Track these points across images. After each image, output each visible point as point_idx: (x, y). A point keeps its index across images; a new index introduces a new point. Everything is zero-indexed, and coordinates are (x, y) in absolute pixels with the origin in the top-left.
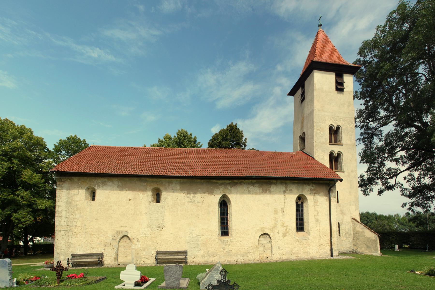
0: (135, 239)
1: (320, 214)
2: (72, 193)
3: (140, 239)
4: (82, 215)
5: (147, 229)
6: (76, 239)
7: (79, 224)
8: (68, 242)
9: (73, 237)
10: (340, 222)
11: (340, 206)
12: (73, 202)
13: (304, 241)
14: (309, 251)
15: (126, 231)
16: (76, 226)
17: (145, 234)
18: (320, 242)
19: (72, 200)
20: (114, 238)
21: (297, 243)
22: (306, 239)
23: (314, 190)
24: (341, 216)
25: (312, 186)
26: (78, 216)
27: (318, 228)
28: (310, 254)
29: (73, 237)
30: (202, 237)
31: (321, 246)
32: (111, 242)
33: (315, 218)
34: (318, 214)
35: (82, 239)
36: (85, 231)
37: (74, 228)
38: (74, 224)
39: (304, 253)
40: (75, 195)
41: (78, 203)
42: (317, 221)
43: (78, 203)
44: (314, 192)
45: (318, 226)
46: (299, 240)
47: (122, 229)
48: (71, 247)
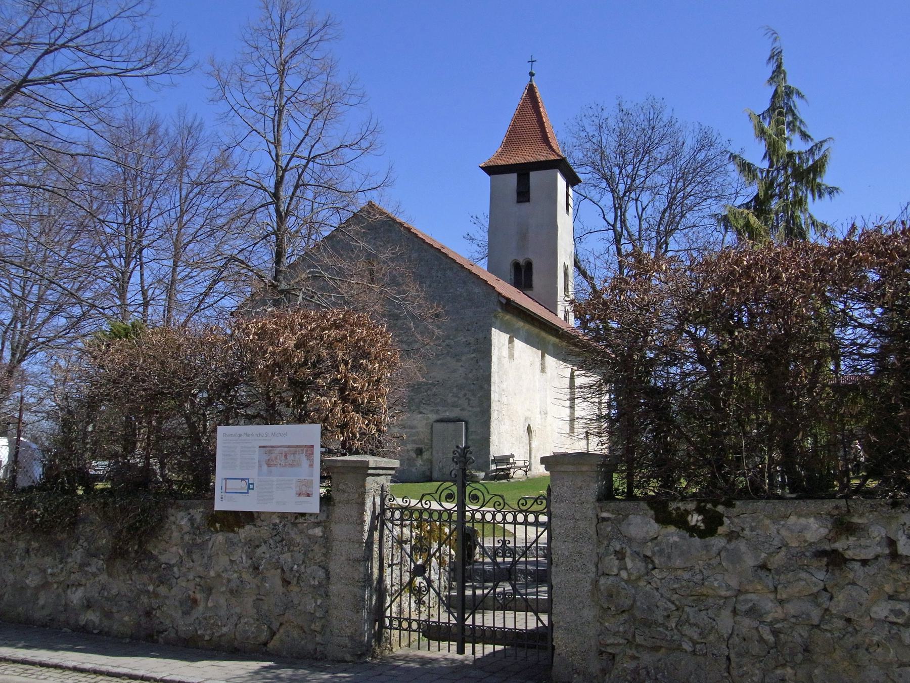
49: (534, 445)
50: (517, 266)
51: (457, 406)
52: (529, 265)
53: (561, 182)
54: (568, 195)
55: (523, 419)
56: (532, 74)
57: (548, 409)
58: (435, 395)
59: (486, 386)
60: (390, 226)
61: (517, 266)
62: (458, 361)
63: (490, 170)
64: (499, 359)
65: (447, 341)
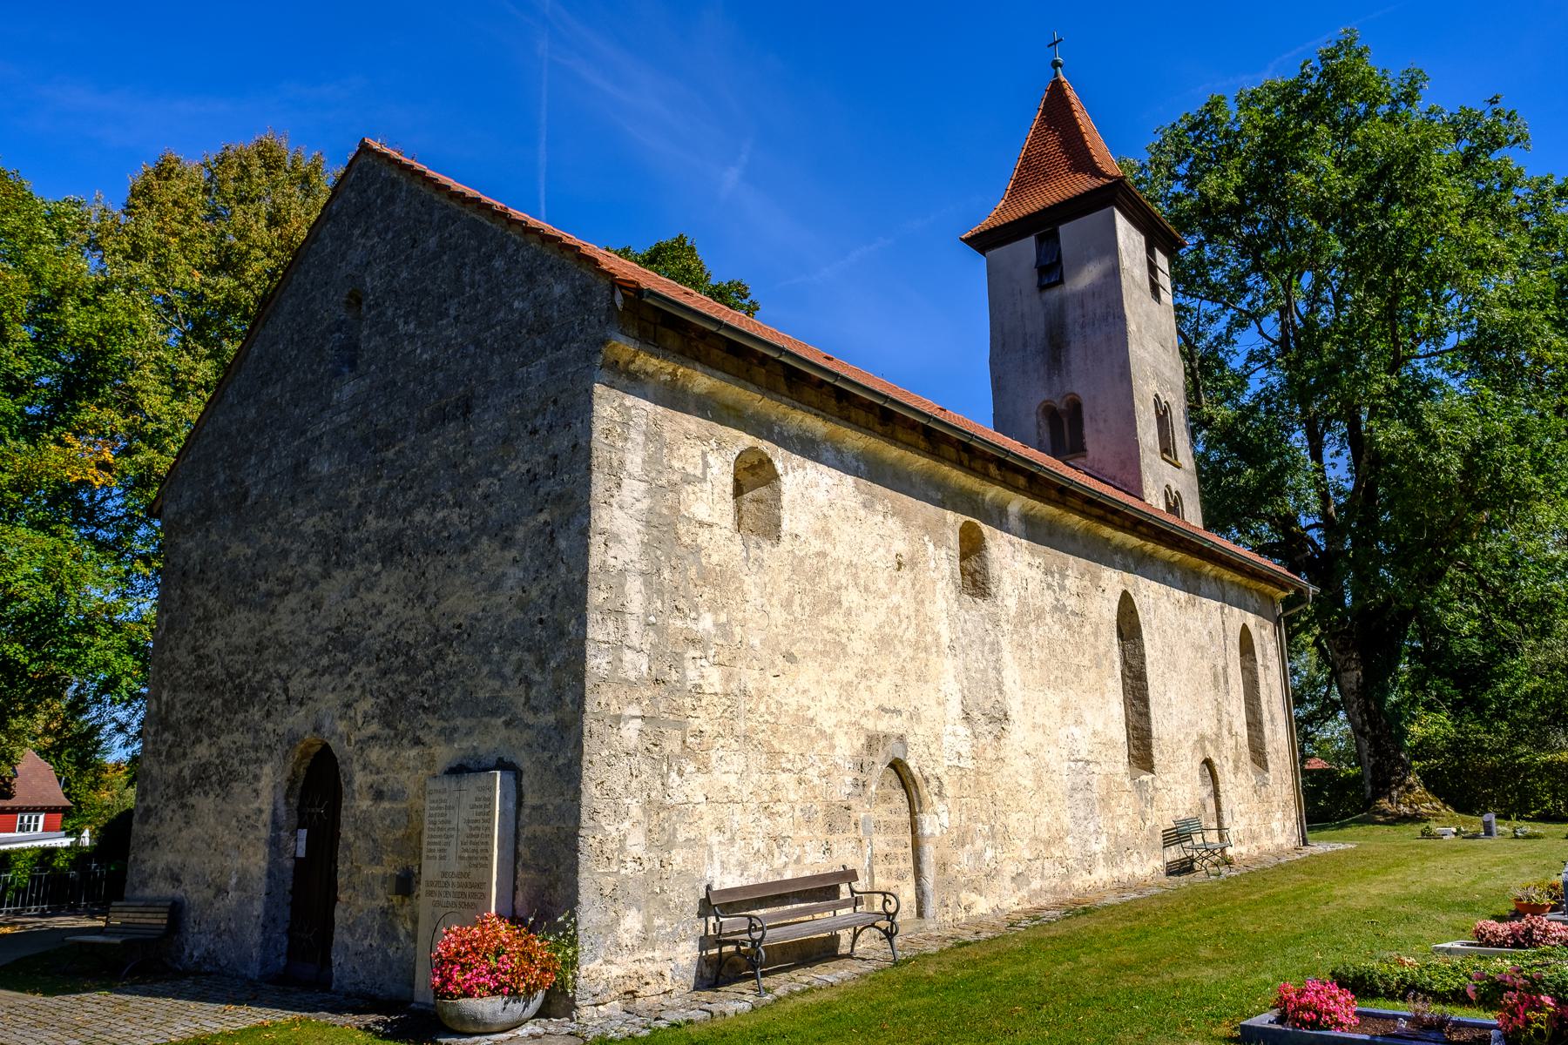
0: (934, 783)
2: (676, 464)
3: (945, 779)
4: (723, 618)
5: (963, 730)
6: (702, 779)
7: (714, 679)
8: (662, 807)
9: (690, 767)
12: (682, 528)
15: (901, 738)
16: (698, 691)
17: (960, 755)
19: (675, 510)
20: (862, 777)
26: (706, 623)
29: (690, 767)
30: (1097, 769)
32: (852, 802)
35: (732, 780)
36: (741, 726)
37: (688, 701)
38: (692, 674)
40: (688, 479)
41: (703, 536)
43: (703, 536)
47: (883, 725)
48: (681, 836)
49: (931, 825)
50: (1051, 415)
51: (494, 713)
52: (1075, 408)
53: (1129, 238)
54: (1153, 268)
55: (847, 746)
56: (1056, 64)
57: (1014, 707)
58: (449, 676)
59: (572, 627)
60: (394, 183)
61: (1051, 415)
62: (507, 543)
63: (983, 242)
64: (664, 529)
65: (484, 482)
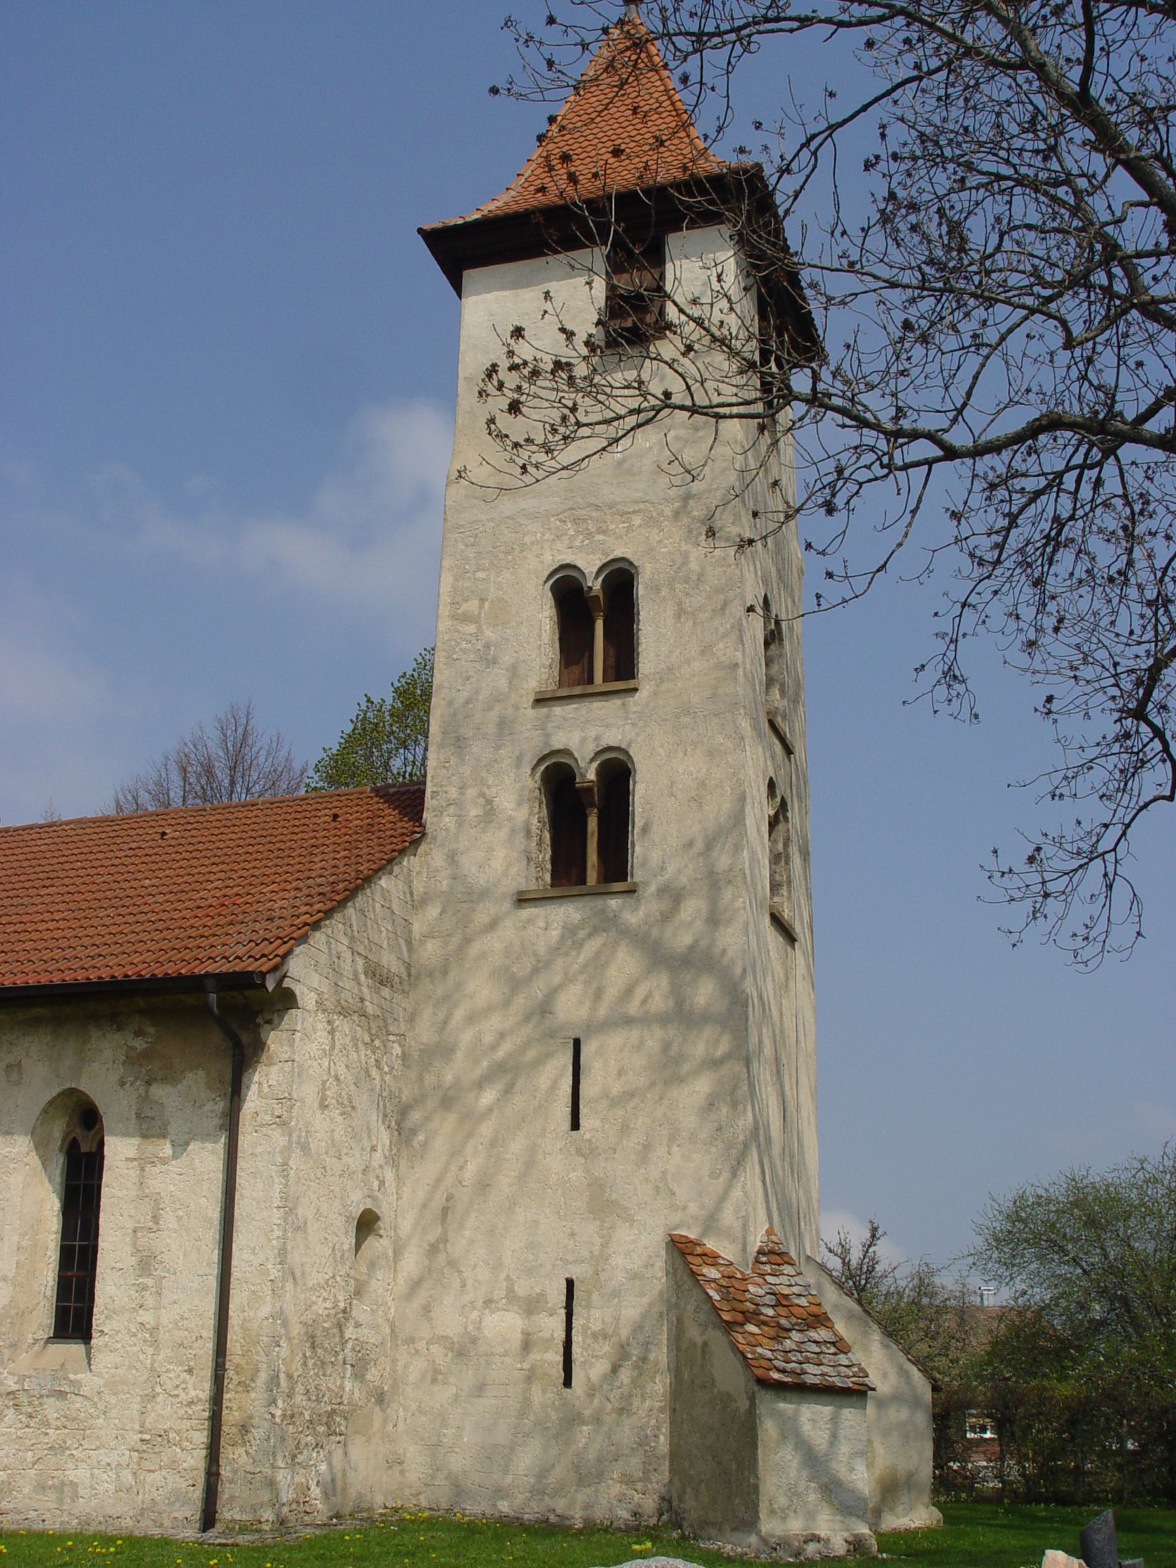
1: (169, 1220)
10: (575, 1272)
11: (588, 1153)
13: (51, 1409)
14: (71, 1475)
18: (150, 1420)
21: (10, 1414)
22: (62, 1395)
23: (146, 1056)
24: (589, 1230)
25: (139, 1033)
27: (147, 1317)
28: (75, 1496)
31: (153, 1442)
33: (136, 1250)
34: (156, 1219)
39: (41, 1487)
42: (146, 1263)
44: (149, 1069)
45: (150, 1301)
46: (24, 1399)
